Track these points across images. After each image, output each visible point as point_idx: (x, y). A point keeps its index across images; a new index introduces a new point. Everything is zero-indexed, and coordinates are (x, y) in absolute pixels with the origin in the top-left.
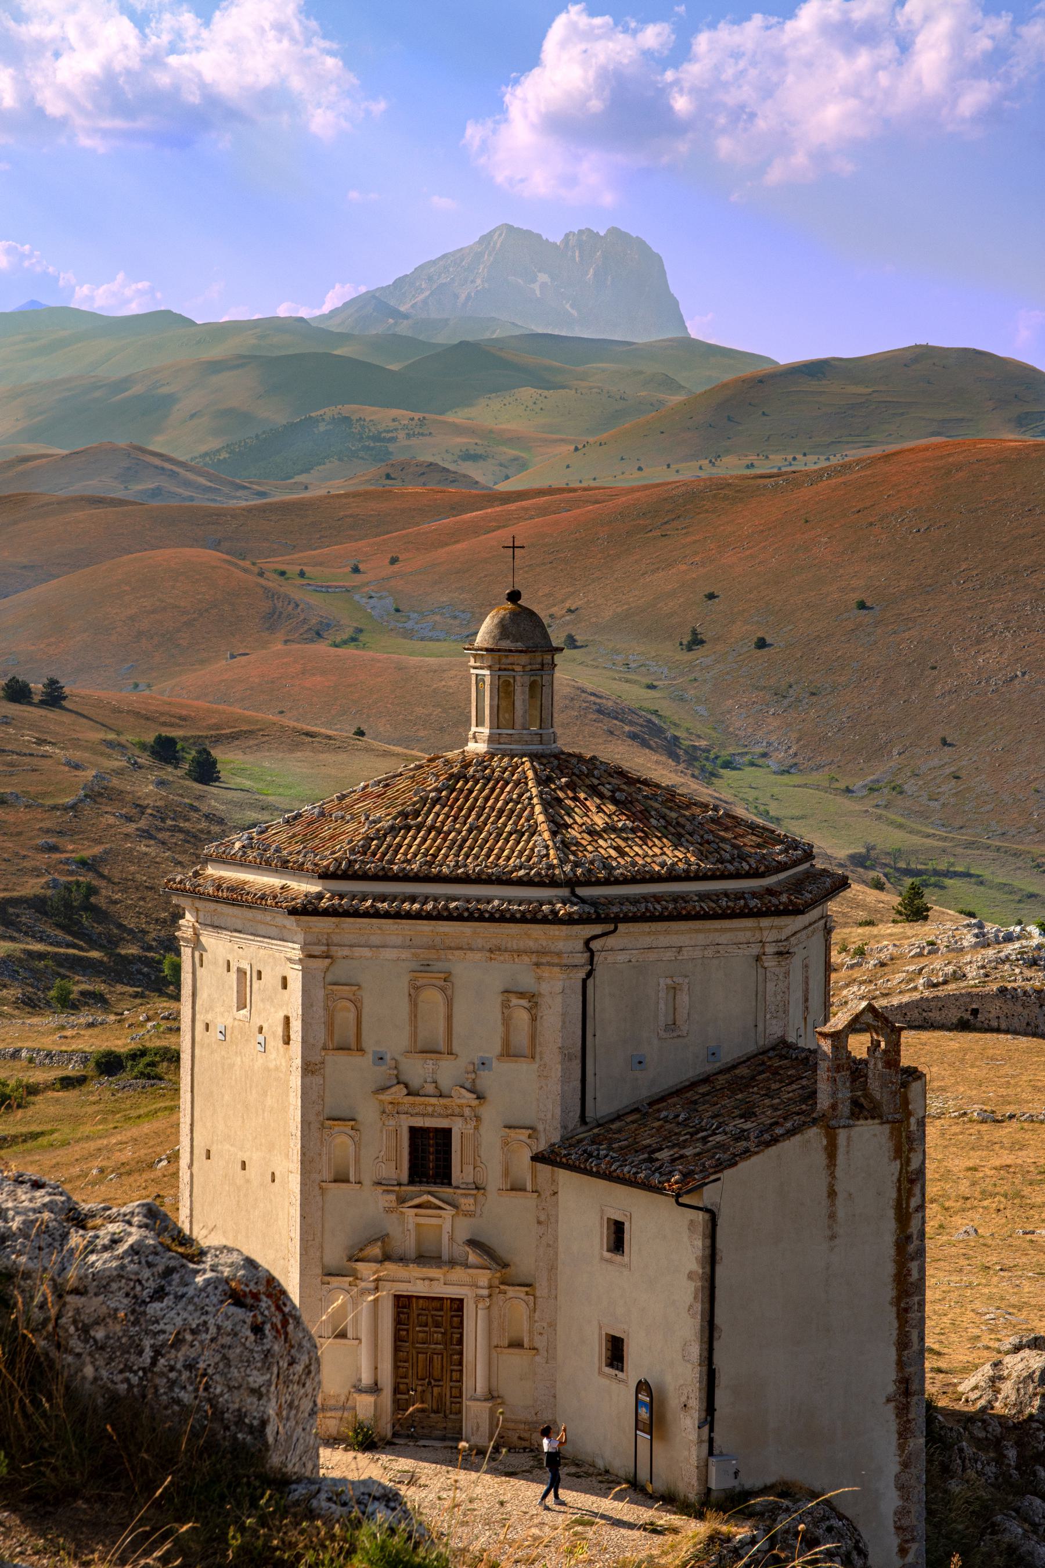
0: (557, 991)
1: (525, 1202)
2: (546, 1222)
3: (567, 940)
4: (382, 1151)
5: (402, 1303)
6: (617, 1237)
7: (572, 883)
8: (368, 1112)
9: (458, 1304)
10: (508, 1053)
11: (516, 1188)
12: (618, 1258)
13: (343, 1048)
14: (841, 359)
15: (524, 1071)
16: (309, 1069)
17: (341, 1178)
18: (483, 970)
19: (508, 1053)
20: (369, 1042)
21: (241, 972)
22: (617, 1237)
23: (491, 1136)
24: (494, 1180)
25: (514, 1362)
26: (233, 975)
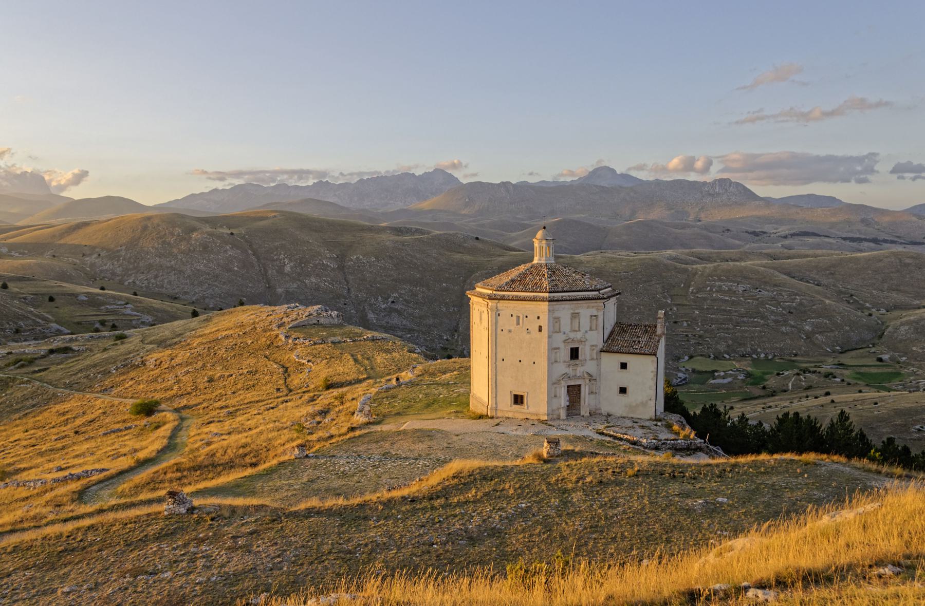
0: (600, 314)
1: (595, 362)
2: (599, 365)
3: (600, 303)
4: (565, 354)
5: (568, 387)
6: (624, 366)
7: (599, 290)
8: (562, 345)
9: (580, 386)
10: (591, 329)
11: (592, 359)
12: (624, 370)
13: (556, 332)
14: (177, 201)
15: (594, 333)
16: (549, 337)
17: (556, 362)
18: (586, 311)
19: (591, 329)
20: (562, 330)
21: (518, 317)
22: (624, 366)
23: (588, 348)
24: (588, 358)
25: (592, 396)
26: (514, 318)
